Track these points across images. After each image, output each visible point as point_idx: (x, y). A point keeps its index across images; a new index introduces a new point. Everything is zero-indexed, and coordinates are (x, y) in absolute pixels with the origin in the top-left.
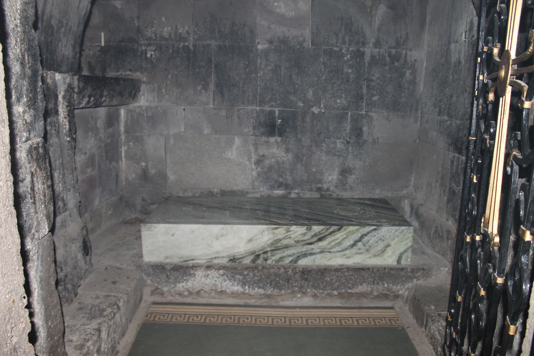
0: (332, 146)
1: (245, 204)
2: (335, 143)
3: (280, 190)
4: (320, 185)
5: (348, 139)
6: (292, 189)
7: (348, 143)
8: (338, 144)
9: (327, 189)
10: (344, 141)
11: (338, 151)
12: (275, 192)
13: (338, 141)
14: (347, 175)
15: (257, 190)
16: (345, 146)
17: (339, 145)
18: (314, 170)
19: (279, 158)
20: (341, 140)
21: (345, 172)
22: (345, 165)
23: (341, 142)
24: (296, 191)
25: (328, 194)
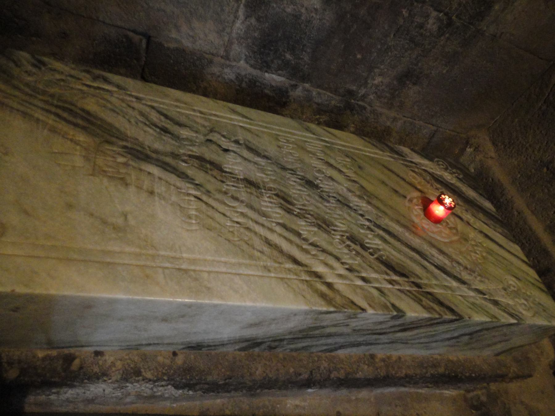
0: (419, 20)
1: (225, 144)
2: (428, 16)
3: (279, 75)
4: (354, 88)
5: (454, 18)
6: (304, 79)
7: (450, 23)
8: (431, 21)
9: (363, 96)
10: (445, 18)
11: (421, 35)
12: (267, 75)
13: (434, 14)
14: (408, 82)
15: (234, 64)
16: (440, 28)
17: (432, 25)
18: (359, 56)
19: (303, 10)
20: (441, 15)
21: (407, 77)
22: (416, 65)
23: (439, 19)
24: (307, 85)
25: (360, 106)
